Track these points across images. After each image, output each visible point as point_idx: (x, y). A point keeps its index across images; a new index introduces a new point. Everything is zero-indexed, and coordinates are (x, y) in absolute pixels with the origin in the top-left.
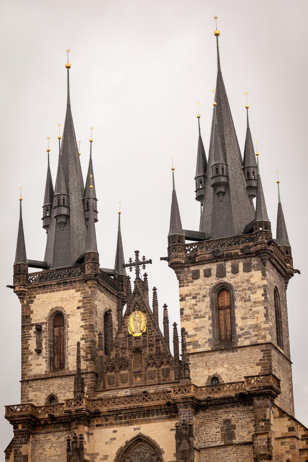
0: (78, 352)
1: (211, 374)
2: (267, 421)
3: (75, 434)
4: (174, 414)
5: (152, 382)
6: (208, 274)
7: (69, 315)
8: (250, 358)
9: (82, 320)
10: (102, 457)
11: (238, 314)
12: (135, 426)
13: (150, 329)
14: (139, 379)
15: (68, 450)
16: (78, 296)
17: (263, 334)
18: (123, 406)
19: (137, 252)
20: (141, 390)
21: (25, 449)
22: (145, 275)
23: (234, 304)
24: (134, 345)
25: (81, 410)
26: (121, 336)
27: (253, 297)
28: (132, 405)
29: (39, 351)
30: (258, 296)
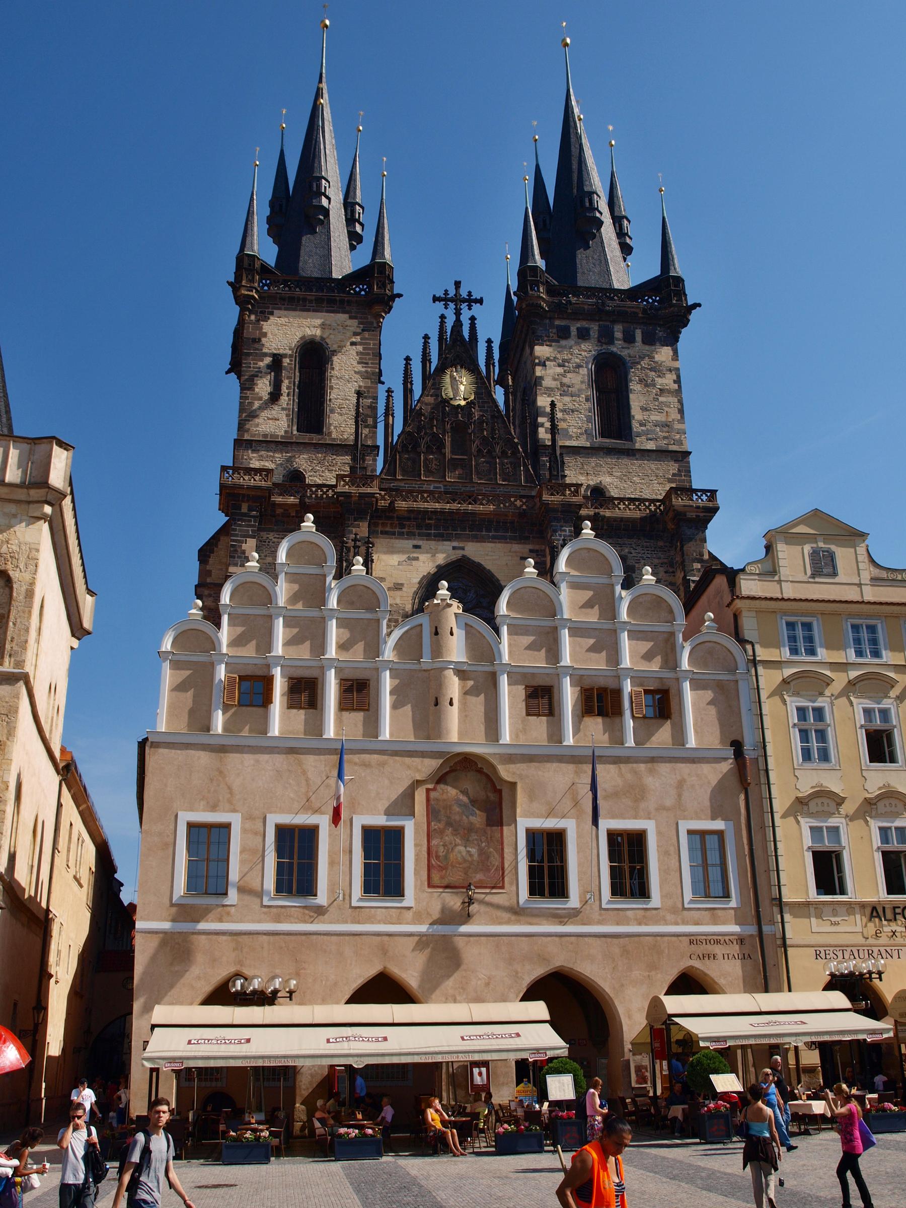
1: (591, 483)
3: (356, 534)
4: (527, 534)
6: (583, 335)
7: (335, 351)
8: (657, 469)
9: (359, 363)
10: (392, 585)
11: (636, 401)
12: (455, 544)
13: (482, 398)
17: (678, 437)
18: (437, 505)
19: (458, 284)
22: (473, 319)
23: (627, 386)
27: (659, 381)
28: (455, 506)
29: (275, 397)
30: (668, 381)
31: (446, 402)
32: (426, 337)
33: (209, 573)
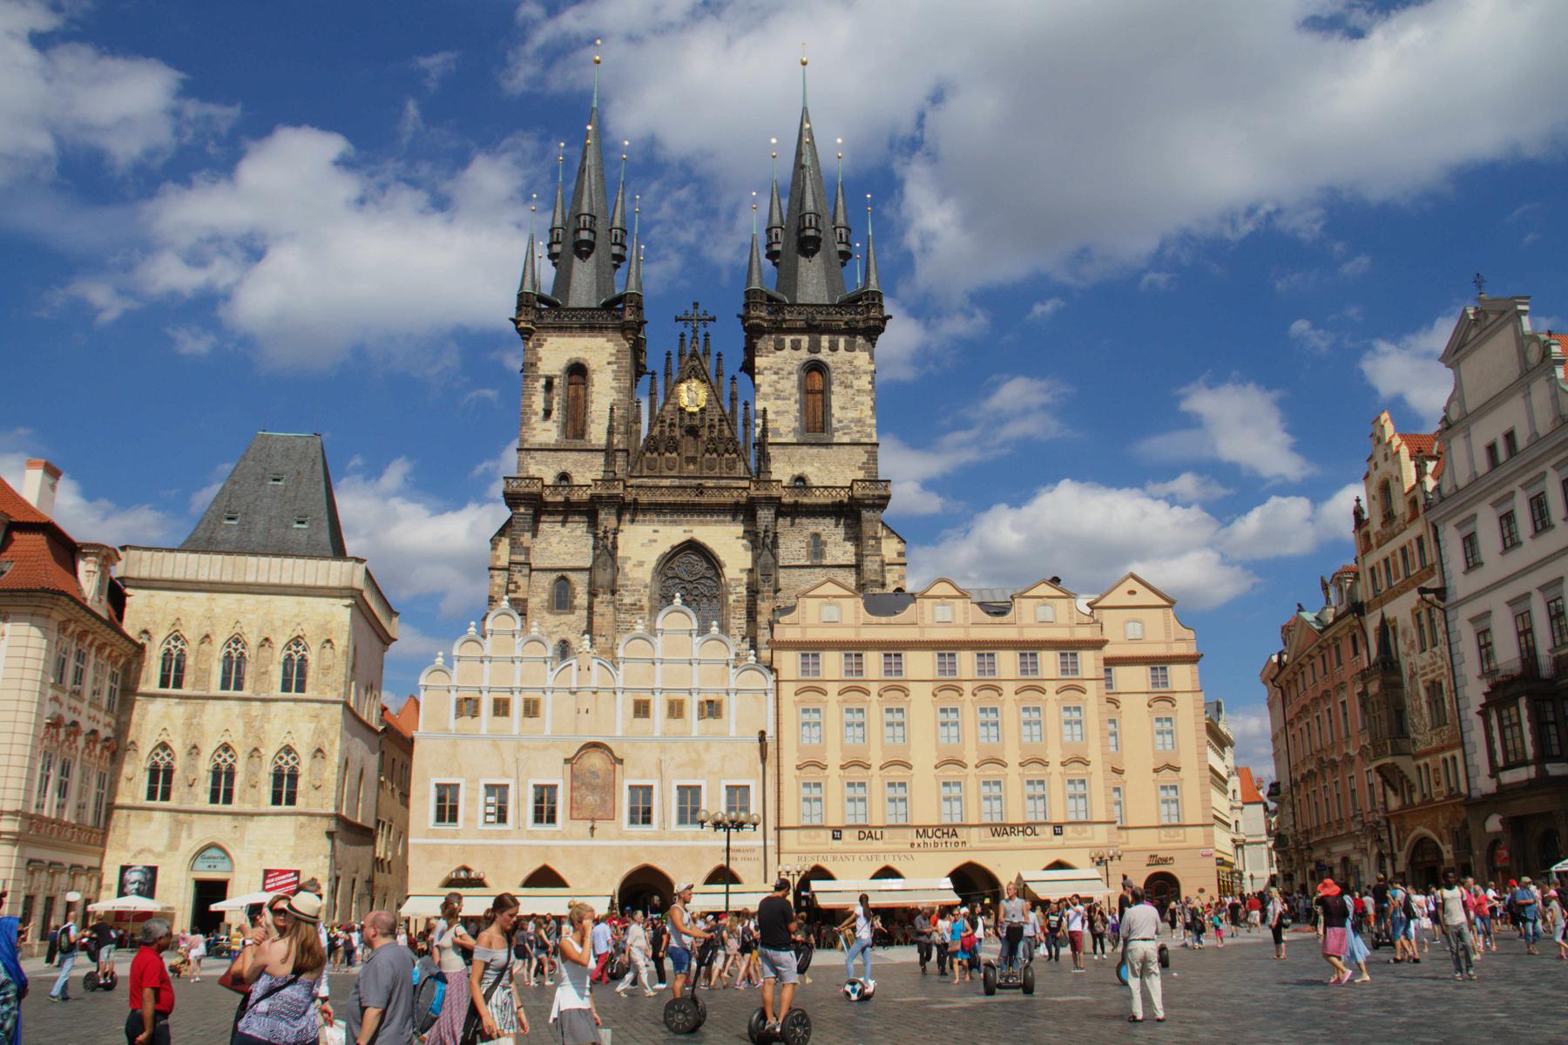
0: (611, 419)
2: (878, 539)
5: (712, 474)
6: (796, 346)
14: (691, 467)
15: (594, 548)
16: (610, 347)
19: (696, 305)
20: (695, 482)
21: (526, 538)
22: (707, 335)
24: (687, 422)
25: (617, 496)
26: (669, 407)
27: (856, 383)
29: (548, 413)
30: (864, 382)
31: (682, 410)
32: (669, 354)
33: (498, 558)
